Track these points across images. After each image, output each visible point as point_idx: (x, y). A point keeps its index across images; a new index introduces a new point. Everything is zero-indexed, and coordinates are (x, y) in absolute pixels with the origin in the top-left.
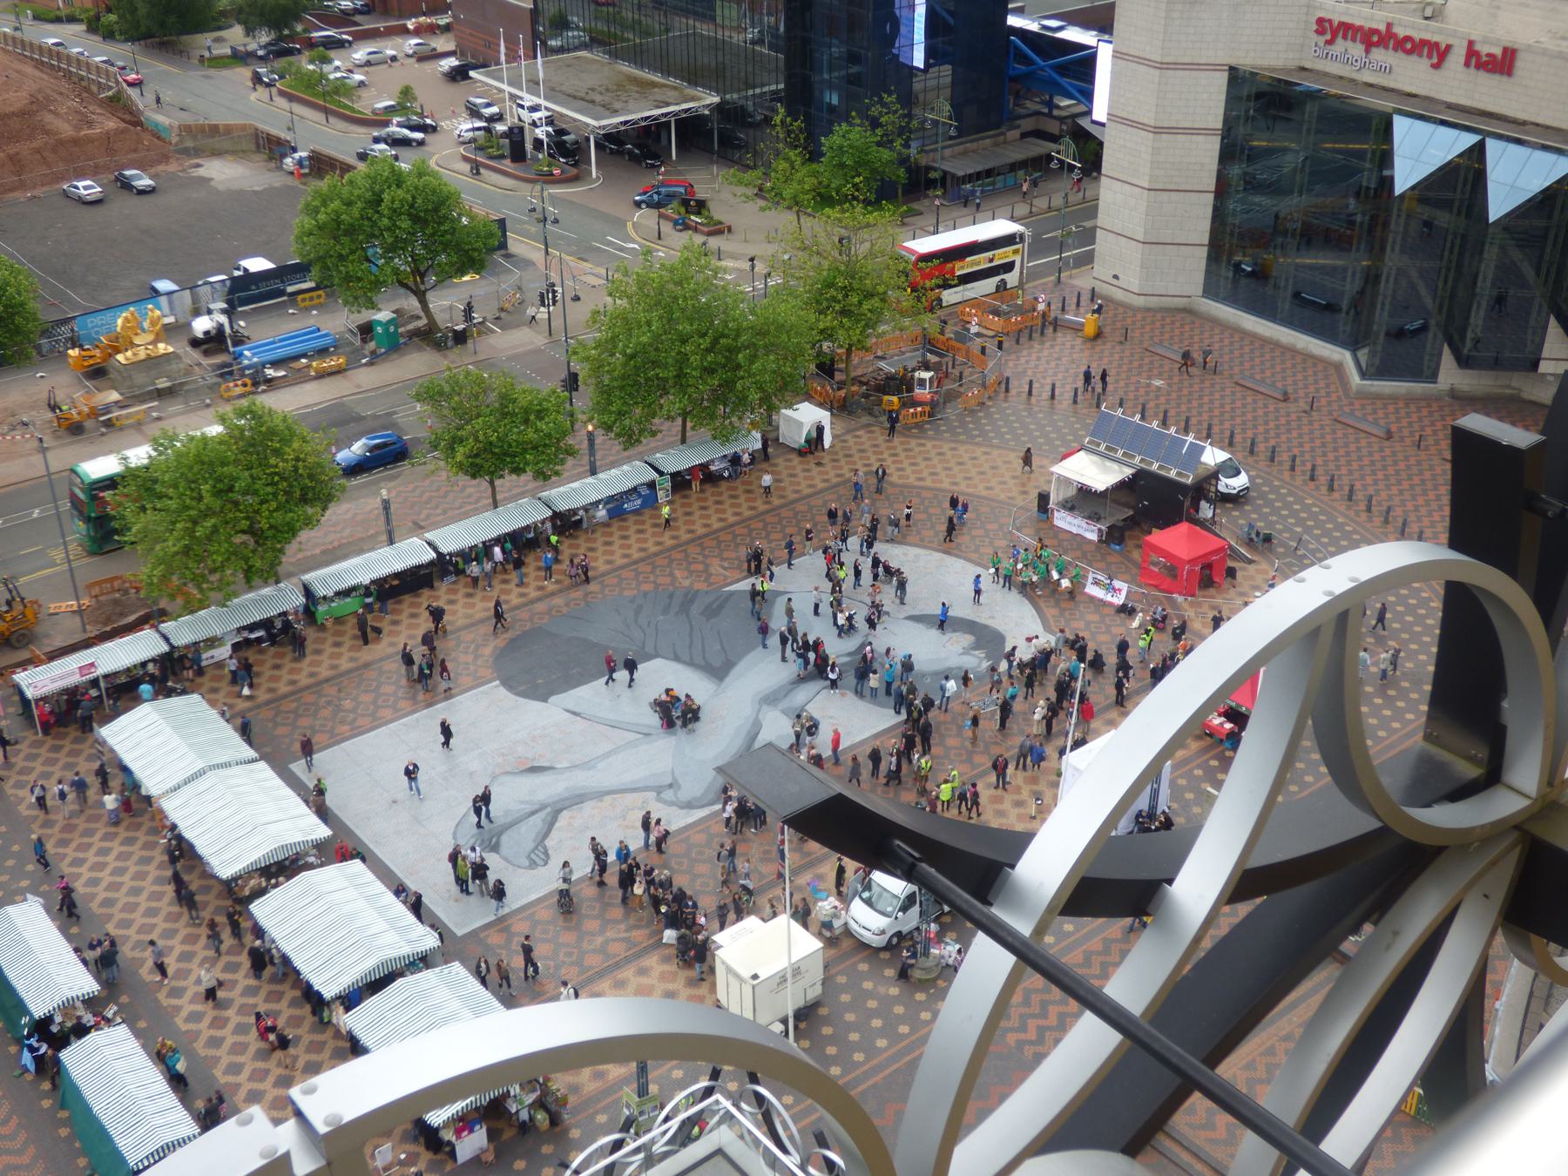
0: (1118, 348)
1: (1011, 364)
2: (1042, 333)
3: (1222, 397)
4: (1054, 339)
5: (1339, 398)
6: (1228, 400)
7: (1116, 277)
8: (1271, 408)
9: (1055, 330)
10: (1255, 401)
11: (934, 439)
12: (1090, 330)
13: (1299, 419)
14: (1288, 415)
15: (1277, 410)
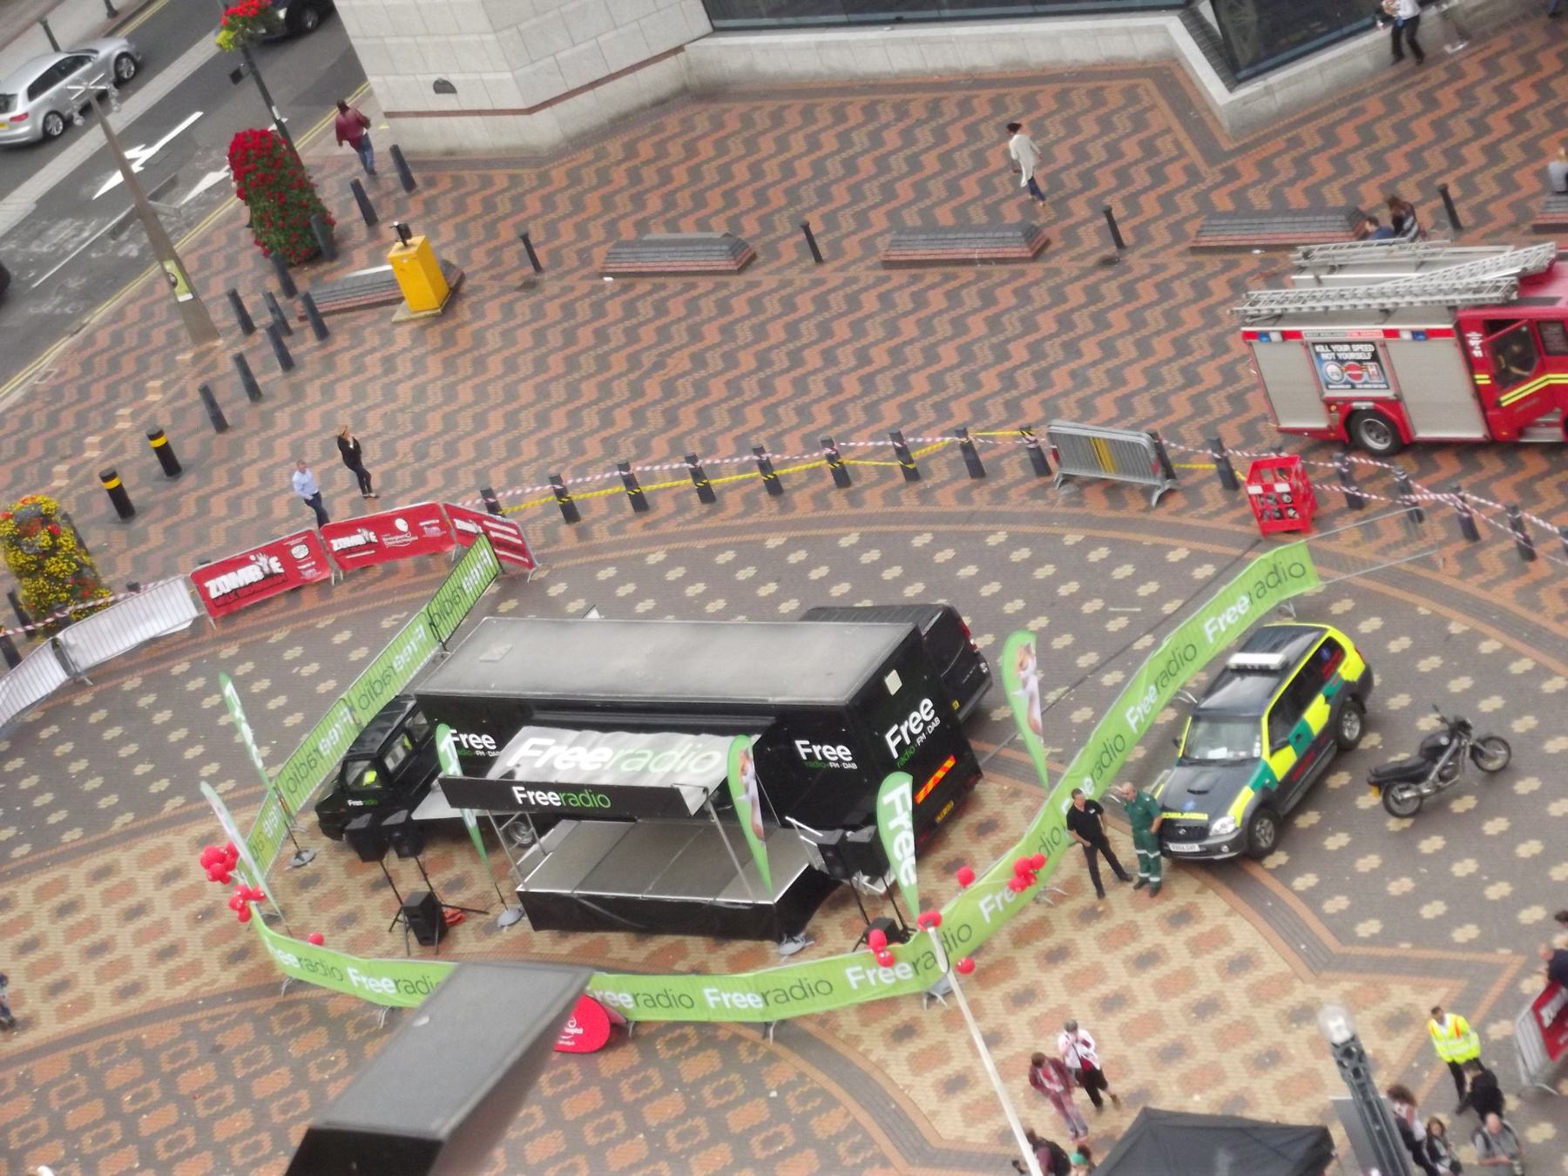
0: (523, 308)
1: (218, 507)
2: (287, 363)
3: (858, 329)
4: (329, 363)
5: (1193, 175)
6: (875, 331)
7: (443, 87)
8: (1005, 297)
9: (322, 333)
10: (953, 297)
11: (40, 866)
12: (421, 293)
13: (1093, 294)
14: (1058, 296)
15: (1023, 295)
